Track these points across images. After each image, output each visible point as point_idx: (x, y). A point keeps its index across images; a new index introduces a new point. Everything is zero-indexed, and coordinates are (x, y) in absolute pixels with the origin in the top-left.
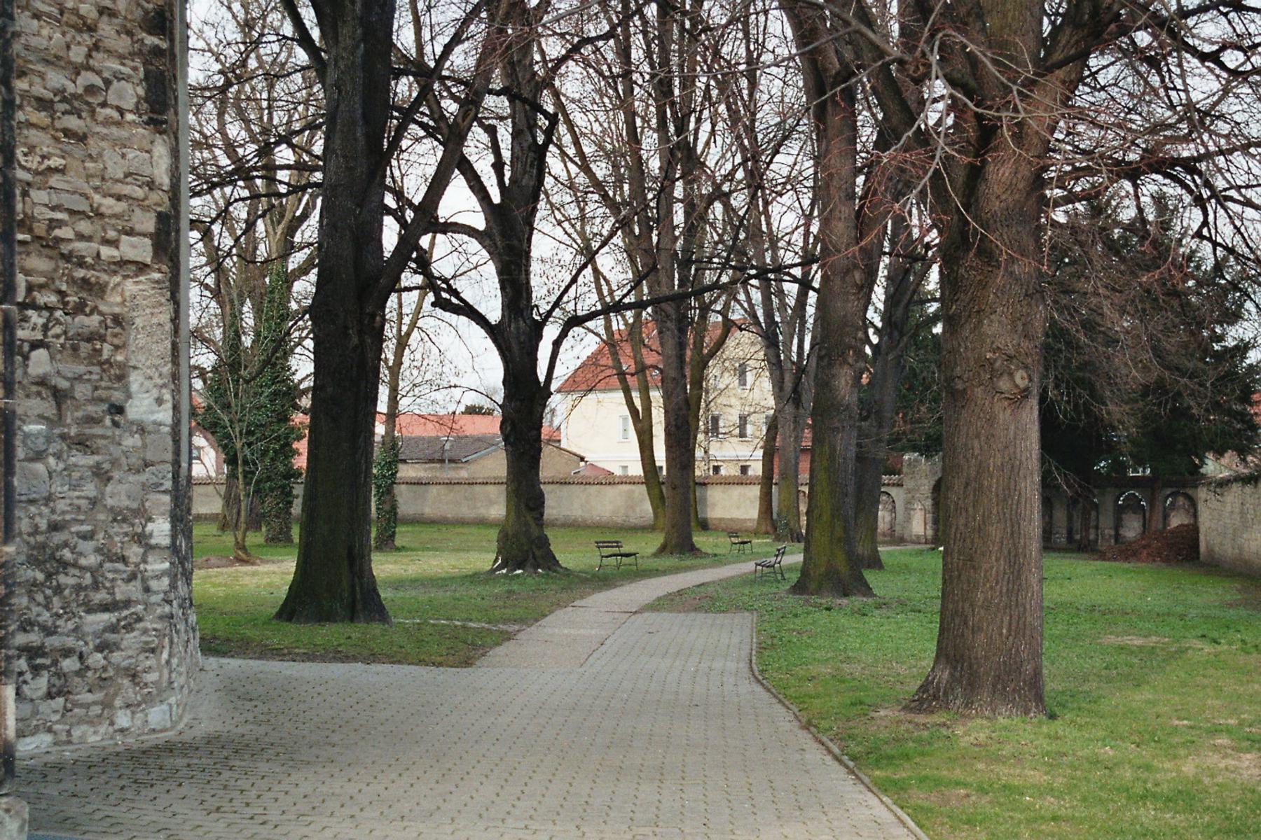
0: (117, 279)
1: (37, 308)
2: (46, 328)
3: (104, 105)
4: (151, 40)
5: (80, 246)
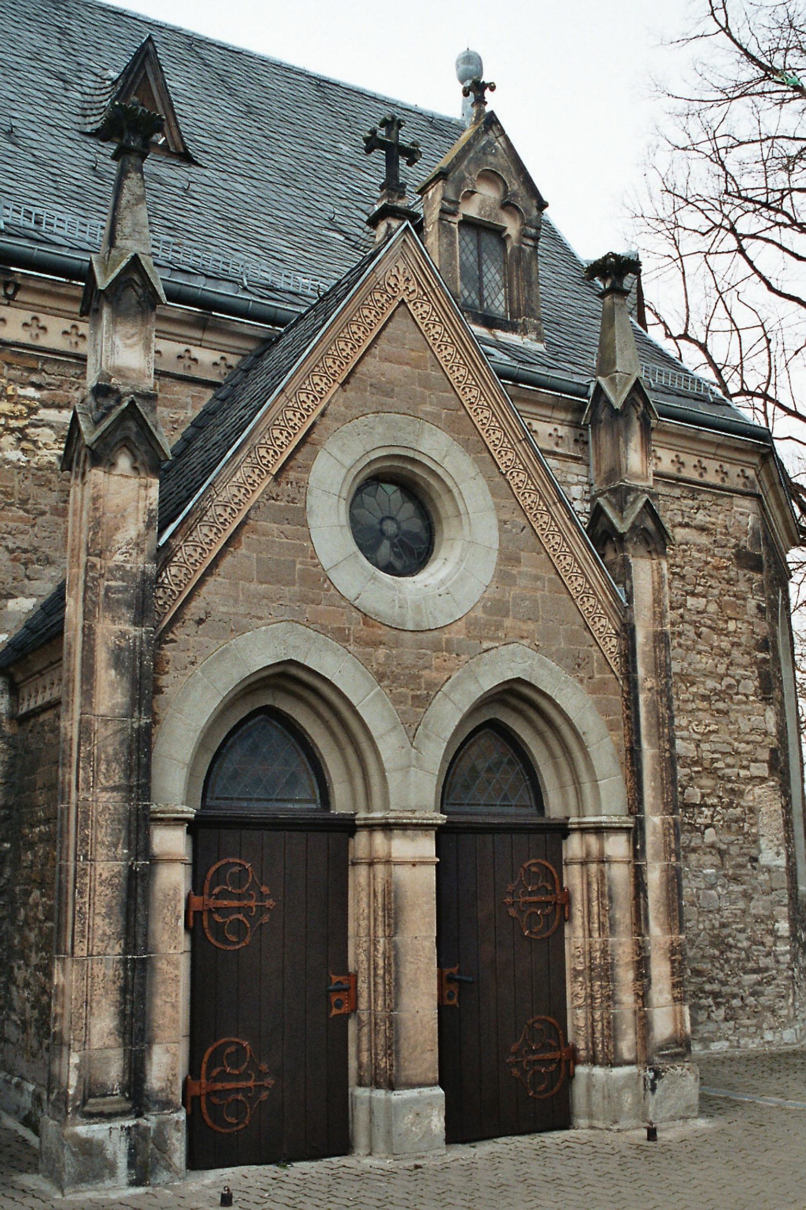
0: (750, 787)
1: (706, 806)
2: (712, 817)
3: (737, 694)
4: (761, 655)
5: (728, 771)
